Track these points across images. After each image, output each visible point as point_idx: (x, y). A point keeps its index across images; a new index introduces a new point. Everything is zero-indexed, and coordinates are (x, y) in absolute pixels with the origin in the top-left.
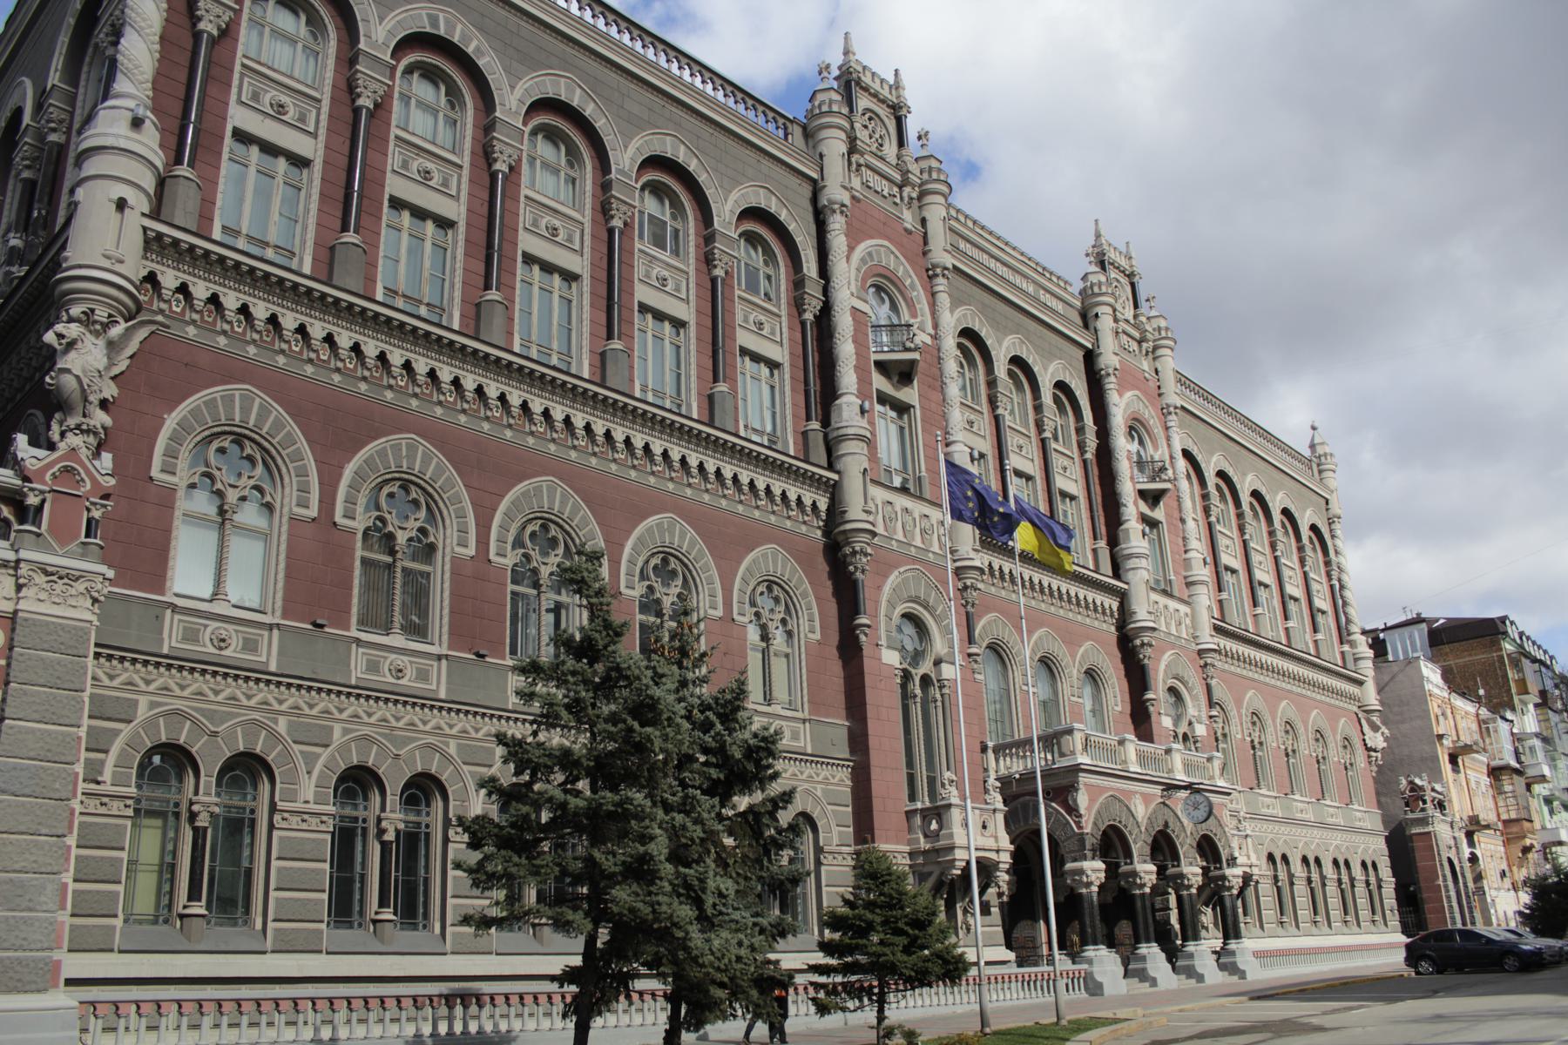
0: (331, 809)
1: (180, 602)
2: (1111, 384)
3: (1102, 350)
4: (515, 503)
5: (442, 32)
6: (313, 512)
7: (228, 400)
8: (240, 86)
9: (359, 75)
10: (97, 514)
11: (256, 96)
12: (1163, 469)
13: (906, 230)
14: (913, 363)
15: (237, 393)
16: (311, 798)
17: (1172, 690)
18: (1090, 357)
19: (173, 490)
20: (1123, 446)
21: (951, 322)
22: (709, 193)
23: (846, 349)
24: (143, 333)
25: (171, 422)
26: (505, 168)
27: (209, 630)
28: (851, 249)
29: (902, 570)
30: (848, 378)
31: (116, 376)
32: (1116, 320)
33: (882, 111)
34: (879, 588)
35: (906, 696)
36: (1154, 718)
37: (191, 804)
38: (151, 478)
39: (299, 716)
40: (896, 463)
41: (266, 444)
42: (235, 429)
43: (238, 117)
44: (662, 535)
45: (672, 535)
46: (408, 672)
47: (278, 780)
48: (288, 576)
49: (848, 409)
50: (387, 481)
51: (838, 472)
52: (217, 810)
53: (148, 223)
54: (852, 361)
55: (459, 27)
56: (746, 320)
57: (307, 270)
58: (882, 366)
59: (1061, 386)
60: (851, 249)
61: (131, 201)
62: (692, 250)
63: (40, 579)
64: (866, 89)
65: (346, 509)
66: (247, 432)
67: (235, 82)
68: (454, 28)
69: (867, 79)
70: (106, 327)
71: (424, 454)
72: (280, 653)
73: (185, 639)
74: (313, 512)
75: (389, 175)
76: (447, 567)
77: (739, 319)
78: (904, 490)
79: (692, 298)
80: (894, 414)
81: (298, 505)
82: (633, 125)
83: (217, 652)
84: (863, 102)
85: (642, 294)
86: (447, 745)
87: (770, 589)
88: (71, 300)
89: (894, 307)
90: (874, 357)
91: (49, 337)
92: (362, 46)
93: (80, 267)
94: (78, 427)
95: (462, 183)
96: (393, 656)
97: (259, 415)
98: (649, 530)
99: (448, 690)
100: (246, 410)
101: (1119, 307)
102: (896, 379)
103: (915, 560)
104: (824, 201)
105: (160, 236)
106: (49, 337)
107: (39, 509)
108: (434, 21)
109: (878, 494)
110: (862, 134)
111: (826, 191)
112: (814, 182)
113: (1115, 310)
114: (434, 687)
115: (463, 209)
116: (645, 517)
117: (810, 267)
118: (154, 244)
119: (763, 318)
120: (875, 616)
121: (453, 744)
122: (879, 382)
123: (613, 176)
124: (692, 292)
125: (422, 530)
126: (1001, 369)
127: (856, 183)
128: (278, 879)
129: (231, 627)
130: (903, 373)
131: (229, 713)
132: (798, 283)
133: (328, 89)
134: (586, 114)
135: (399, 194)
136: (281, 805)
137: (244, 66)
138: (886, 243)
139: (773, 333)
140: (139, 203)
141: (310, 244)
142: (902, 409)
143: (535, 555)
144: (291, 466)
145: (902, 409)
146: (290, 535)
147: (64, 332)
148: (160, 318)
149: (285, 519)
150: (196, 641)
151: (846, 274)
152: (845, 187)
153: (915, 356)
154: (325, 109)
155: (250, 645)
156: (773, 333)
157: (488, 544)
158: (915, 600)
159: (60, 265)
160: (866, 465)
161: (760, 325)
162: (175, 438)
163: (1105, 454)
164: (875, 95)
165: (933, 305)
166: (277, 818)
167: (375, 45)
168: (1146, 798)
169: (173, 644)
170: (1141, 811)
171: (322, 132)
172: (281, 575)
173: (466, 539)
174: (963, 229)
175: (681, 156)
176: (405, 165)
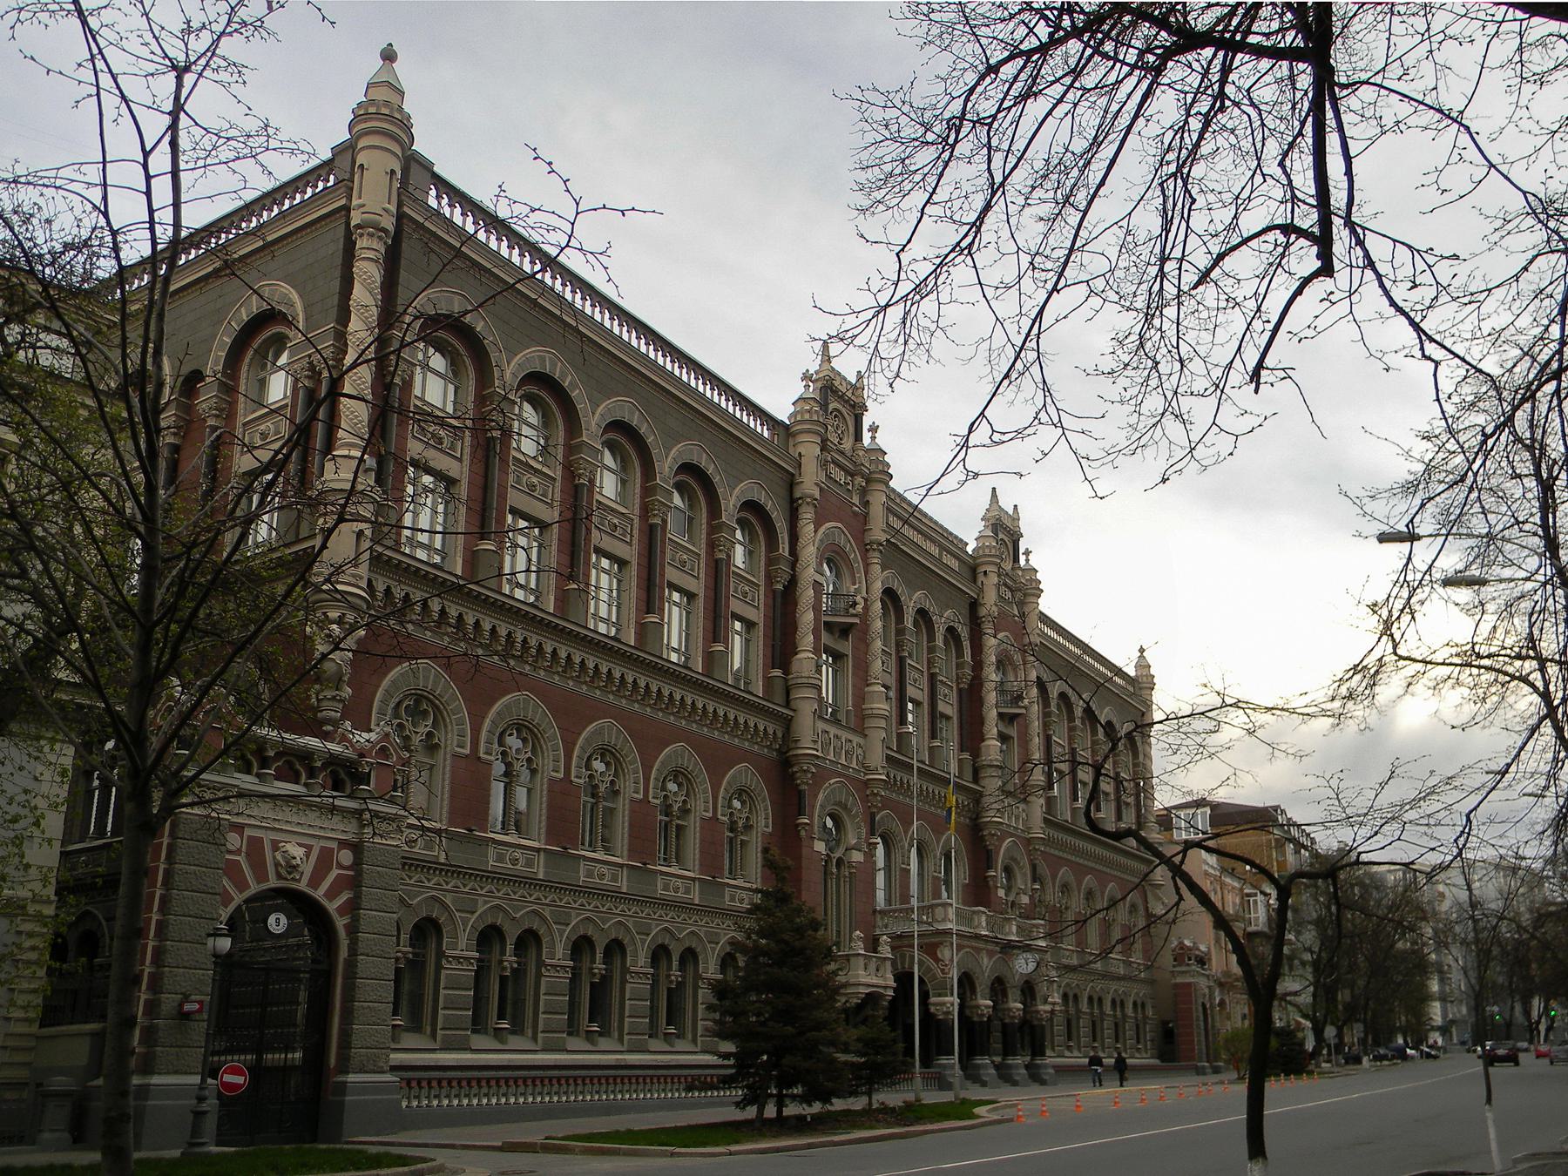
2: (988, 629)
3: (985, 601)
12: (1020, 697)
17: (1008, 870)
18: (974, 605)
20: (992, 675)
21: (878, 587)
23: (807, 618)
29: (832, 781)
30: (806, 640)
34: (816, 796)
35: (826, 872)
45: (683, 758)
48: (452, 797)
49: (805, 658)
65: (487, 748)
74: (467, 751)
76: (545, 786)
78: (835, 721)
79: (702, 575)
81: (458, 746)
87: (740, 795)
90: (824, 619)
98: (669, 756)
99: (545, 872)
100: (435, 683)
103: (840, 775)
104: (797, 494)
109: (821, 725)
117: (784, 549)
120: (811, 818)
122: (825, 638)
124: (702, 571)
126: (909, 622)
130: (844, 631)
132: (770, 562)
138: (840, 525)
139: (753, 601)
145: (838, 657)
151: (809, 552)
158: (839, 804)
165: (866, 573)
173: (559, 767)
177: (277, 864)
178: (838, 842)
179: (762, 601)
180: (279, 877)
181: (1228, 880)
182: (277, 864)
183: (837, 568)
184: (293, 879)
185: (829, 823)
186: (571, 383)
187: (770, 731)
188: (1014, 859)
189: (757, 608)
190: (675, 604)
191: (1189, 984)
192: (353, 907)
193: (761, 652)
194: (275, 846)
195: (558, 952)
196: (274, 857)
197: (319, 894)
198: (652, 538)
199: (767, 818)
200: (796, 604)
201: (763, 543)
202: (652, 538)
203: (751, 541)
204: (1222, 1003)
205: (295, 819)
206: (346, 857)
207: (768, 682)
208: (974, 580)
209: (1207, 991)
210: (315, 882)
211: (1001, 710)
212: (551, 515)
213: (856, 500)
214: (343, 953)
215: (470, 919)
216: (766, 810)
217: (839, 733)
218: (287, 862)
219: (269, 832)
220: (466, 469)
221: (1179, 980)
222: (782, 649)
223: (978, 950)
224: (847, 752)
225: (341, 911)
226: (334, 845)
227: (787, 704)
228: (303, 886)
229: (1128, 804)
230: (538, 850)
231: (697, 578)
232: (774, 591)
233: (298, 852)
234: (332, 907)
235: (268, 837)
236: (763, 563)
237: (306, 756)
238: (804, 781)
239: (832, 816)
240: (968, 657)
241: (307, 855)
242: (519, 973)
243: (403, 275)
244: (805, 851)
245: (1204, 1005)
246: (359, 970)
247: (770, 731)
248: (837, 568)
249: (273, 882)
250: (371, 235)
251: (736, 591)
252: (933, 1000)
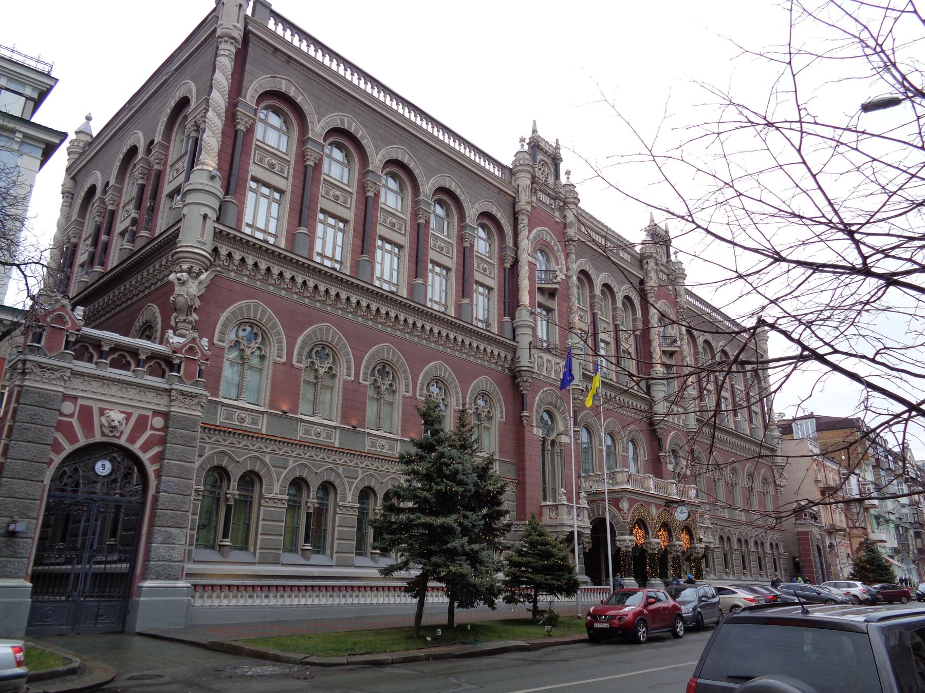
0: (287, 497)
1: (225, 401)
4: (372, 356)
5: (346, 127)
6: (284, 360)
7: (248, 307)
8: (255, 155)
9: (308, 150)
10: (203, 368)
11: (261, 160)
12: (675, 341)
13: (556, 222)
14: (555, 289)
15: (252, 304)
16: (278, 492)
17: (673, 451)
19: (223, 349)
21: (575, 267)
22: (465, 205)
23: (524, 283)
25: (223, 318)
26: (372, 195)
27: (237, 414)
28: (530, 232)
29: (545, 389)
30: (525, 298)
32: (657, 264)
33: (549, 161)
34: (534, 398)
36: (664, 465)
37: (226, 494)
39: (274, 454)
40: (545, 338)
41: (264, 328)
43: (254, 170)
44: (436, 372)
45: (441, 371)
46: (322, 434)
47: (264, 484)
50: (316, 345)
51: (518, 342)
52: (237, 497)
53: (217, 225)
54: (528, 289)
55: (354, 124)
56: (478, 267)
57: (283, 246)
58: (541, 290)
59: (627, 298)
60: (530, 232)
62: (455, 233)
63: (181, 397)
64: (542, 150)
67: (253, 153)
68: (351, 125)
69: (542, 145)
70: (198, 275)
71: (333, 332)
72: (268, 425)
73: (226, 419)
74: (284, 360)
75: (320, 198)
77: (475, 267)
79: (454, 256)
80: (544, 313)
82: (431, 172)
84: (540, 157)
85: (432, 255)
86: (338, 468)
88: (180, 258)
89: (548, 260)
90: (537, 286)
91: (172, 277)
92: (310, 135)
93: (187, 246)
94: (185, 321)
95: (353, 202)
96: (316, 427)
97: (261, 314)
98: (431, 368)
99: (340, 443)
101: (659, 259)
102: (547, 296)
103: (551, 385)
105: (221, 231)
106: (172, 277)
107: (180, 365)
108: (342, 121)
110: (538, 174)
111: (521, 203)
112: (514, 198)
113: (656, 260)
114: (333, 441)
115: (353, 214)
116: (429, 363)
118: (218, 234)
119: (486, 266)
120: (531, 411)
121: (341, 468)
122: (539, 298)
123: (421, 197)
124: (455, 254)
125: (330, 368)
127: (534, 199)
128: (262, 530)
130: (552, 294)
132: (502, 248)
133: (293, 156)
134: (410, 167)
135: (324, 207)
136: (265, 495)
137: (256, 145)
138: (546, 229)
139: (490, 273)
140: (212, 215)
141: (284, 232)
142: (549, 310)
143: (379, 380)
144: (275, 338)
145: (549, 310)
146: (274, 370)
147: (181, 278)
148: (219, 269)
149: (271, 363)
150: (231, 419)
151: (525, 243)
152: (528, 203)
153: (557, 286)
154: (292, 166)
155: (254, 422)
156: (490, 273)
157: (359, 375)
158: (550, 404)
159: (176, 243)
160: (531, 339)
161: (485, 270)
162: (225, 326)
163: (646, 330)
164: (546, 153)
166: (262, 501)
167: (315, 134)
168: (658, 507)
169: (222, 420)
170: (654, 511)
171: (291, 177)
172: (269, 389)
173: (350, 373)
174: (585, 219)
175: (453, 187)
176: (327, 193)
177: (102, 426)
178: (553, 430)
179: (496, 275)
180: (103, 434)
181: (828, 464)
182: (102, 426)
183: (546, 255)
184: (114, 436)
185: (546, 416)
186: (362, 135)
187: (503, 356)
188: (676, 444)
189: (494, 278)
190: (437, 274)
191: (807, 532)
192: (160, 457)
193: (496, 306)
194: (102, 412)
195: (349, 497)
196: (100, 421)
197: (135, 448)
198: (419, 233)
199: (501, 412)
200: (518, 276)
201: (496, 239)
202: (419, 233)
203: (489, 238)
204: (831, 546)
205: (120, 394)
206: (158, 422)
207: (501, 324)
208: (642, 268)
209: (819, 537)
210: (132, 439)
211: (663, 349)
212: (350, 215)
213: (557, 214)
214: (152, 491)
215: (282, 473)
216: (501, 407)
217: (550, 358)
218: (109, 424)
219: (97, 402)
220: (290, 184)
221: (800, 529)
222: (510, 303)
223: (649, 504)
224: (555, 371)
225: (153, 460)
226: (150, 414)
227: (514, 339)
228: (122, 441)
229: (756, 413)
230: (335, 428)
231: (451, 258)
232: (505, 269)
233: (116, 416)
234: (145, 457)
235: (96, 407)
236: (496, 251)
237: (134, 352)
238: (525, 388)
239: (548, 412)
240: (639, 314)
241: (127, 420)
242: (321, 512)
243: (248, 66)
244: (527, 435)
245: (818, 547)
246: (159, 503)
247: (503, 356)
248: (546, 255)
249: (98, 438)
250: (226, 42)
251: (478, 268)
252: (618, 538)
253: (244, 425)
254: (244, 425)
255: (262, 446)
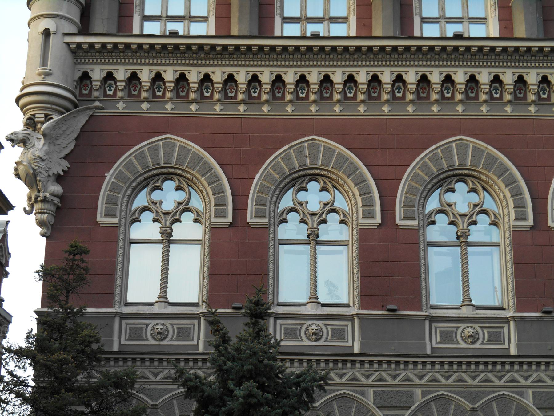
24: (82, 119)
25: (110, 177)
31: (67, 155)
38: (98, 222)
42: (163, 170)
61: (52, 29)
66: (171, 170)
73: (131, 338)
81: (216, 216)
83: (157, 343)
105: (79, 45)
129: (167, 322)
131: (165, 390)
148: (97, 104)
150: (140, 338)
155: (184, 334)
162: (114, 188)
169: (123, 342)
253: (165, 342)
254: (165, 342)
255: (543, 376)
